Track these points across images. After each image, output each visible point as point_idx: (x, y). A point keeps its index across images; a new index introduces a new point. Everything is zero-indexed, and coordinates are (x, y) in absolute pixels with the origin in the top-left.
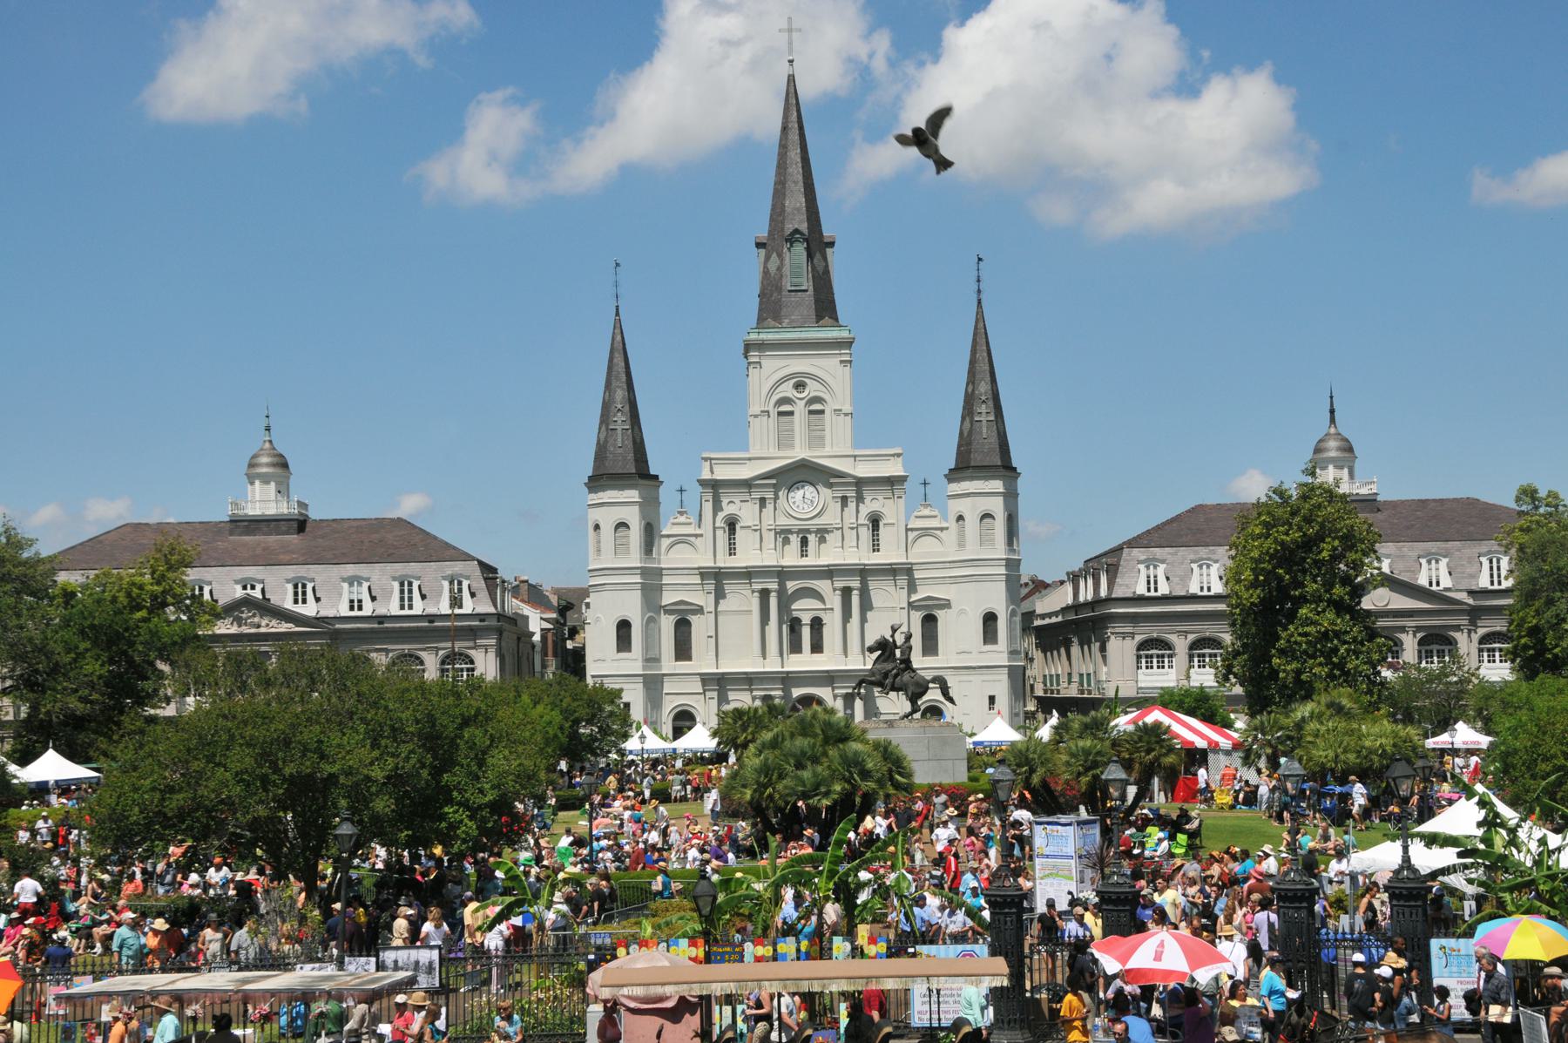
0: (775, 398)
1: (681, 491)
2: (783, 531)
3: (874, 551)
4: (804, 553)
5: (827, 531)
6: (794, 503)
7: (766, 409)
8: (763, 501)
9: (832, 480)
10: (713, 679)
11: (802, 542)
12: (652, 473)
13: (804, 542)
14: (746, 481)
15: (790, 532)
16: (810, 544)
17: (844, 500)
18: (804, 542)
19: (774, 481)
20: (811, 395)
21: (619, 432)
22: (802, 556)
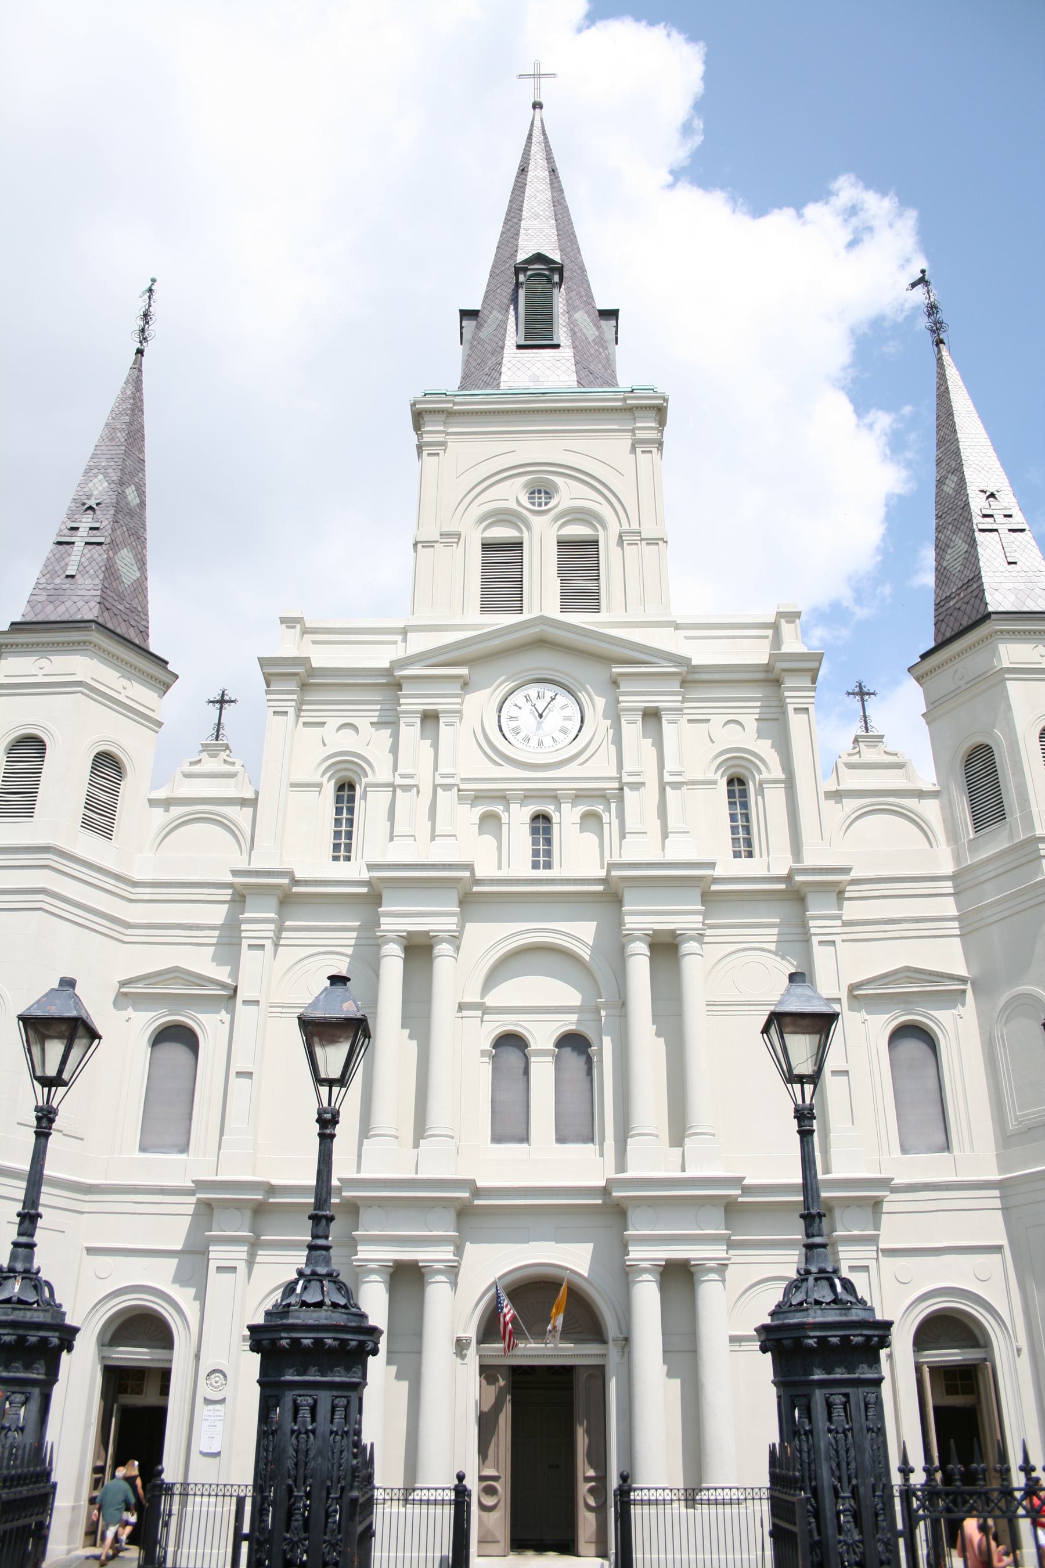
0: (477, 510)
1: (222, 701)
2: (478, 797)
3: (737, 855)
4: (542, 856)
5: (603, 796)
6: (516, 731)
7: (453, 529)
8: (430, 718)
9: (617, 670)
10: (237, 1205)
11: (534, 831)
12: (152, 650)
13: (541, 823)
14: (388, 672)
15: (503, 798)
16: (555, 828)
17: (652, 716)
18: (541, 823)
19: (463, 671)
20: (562, 506)
21: (79, 544)
22: (535, 865)
